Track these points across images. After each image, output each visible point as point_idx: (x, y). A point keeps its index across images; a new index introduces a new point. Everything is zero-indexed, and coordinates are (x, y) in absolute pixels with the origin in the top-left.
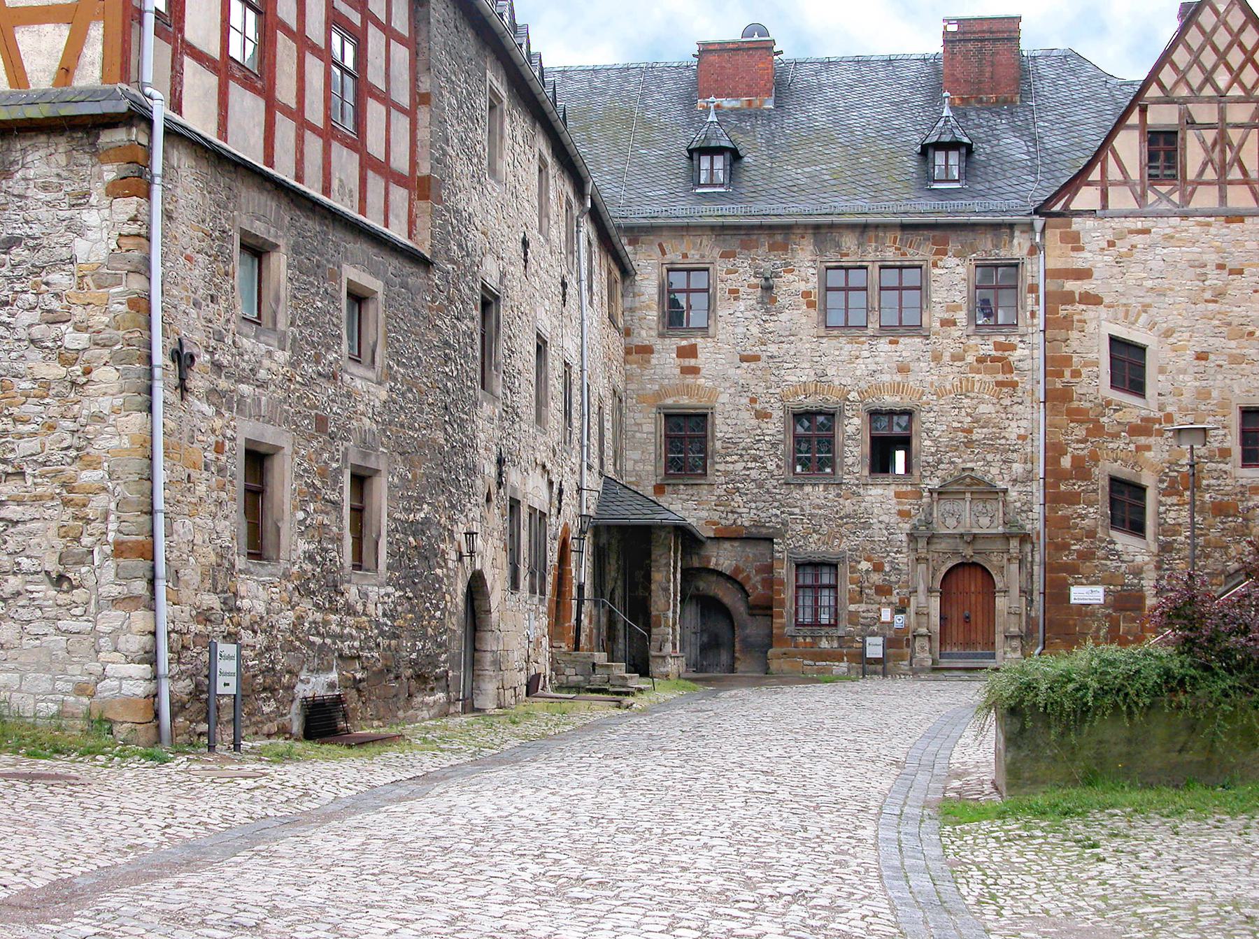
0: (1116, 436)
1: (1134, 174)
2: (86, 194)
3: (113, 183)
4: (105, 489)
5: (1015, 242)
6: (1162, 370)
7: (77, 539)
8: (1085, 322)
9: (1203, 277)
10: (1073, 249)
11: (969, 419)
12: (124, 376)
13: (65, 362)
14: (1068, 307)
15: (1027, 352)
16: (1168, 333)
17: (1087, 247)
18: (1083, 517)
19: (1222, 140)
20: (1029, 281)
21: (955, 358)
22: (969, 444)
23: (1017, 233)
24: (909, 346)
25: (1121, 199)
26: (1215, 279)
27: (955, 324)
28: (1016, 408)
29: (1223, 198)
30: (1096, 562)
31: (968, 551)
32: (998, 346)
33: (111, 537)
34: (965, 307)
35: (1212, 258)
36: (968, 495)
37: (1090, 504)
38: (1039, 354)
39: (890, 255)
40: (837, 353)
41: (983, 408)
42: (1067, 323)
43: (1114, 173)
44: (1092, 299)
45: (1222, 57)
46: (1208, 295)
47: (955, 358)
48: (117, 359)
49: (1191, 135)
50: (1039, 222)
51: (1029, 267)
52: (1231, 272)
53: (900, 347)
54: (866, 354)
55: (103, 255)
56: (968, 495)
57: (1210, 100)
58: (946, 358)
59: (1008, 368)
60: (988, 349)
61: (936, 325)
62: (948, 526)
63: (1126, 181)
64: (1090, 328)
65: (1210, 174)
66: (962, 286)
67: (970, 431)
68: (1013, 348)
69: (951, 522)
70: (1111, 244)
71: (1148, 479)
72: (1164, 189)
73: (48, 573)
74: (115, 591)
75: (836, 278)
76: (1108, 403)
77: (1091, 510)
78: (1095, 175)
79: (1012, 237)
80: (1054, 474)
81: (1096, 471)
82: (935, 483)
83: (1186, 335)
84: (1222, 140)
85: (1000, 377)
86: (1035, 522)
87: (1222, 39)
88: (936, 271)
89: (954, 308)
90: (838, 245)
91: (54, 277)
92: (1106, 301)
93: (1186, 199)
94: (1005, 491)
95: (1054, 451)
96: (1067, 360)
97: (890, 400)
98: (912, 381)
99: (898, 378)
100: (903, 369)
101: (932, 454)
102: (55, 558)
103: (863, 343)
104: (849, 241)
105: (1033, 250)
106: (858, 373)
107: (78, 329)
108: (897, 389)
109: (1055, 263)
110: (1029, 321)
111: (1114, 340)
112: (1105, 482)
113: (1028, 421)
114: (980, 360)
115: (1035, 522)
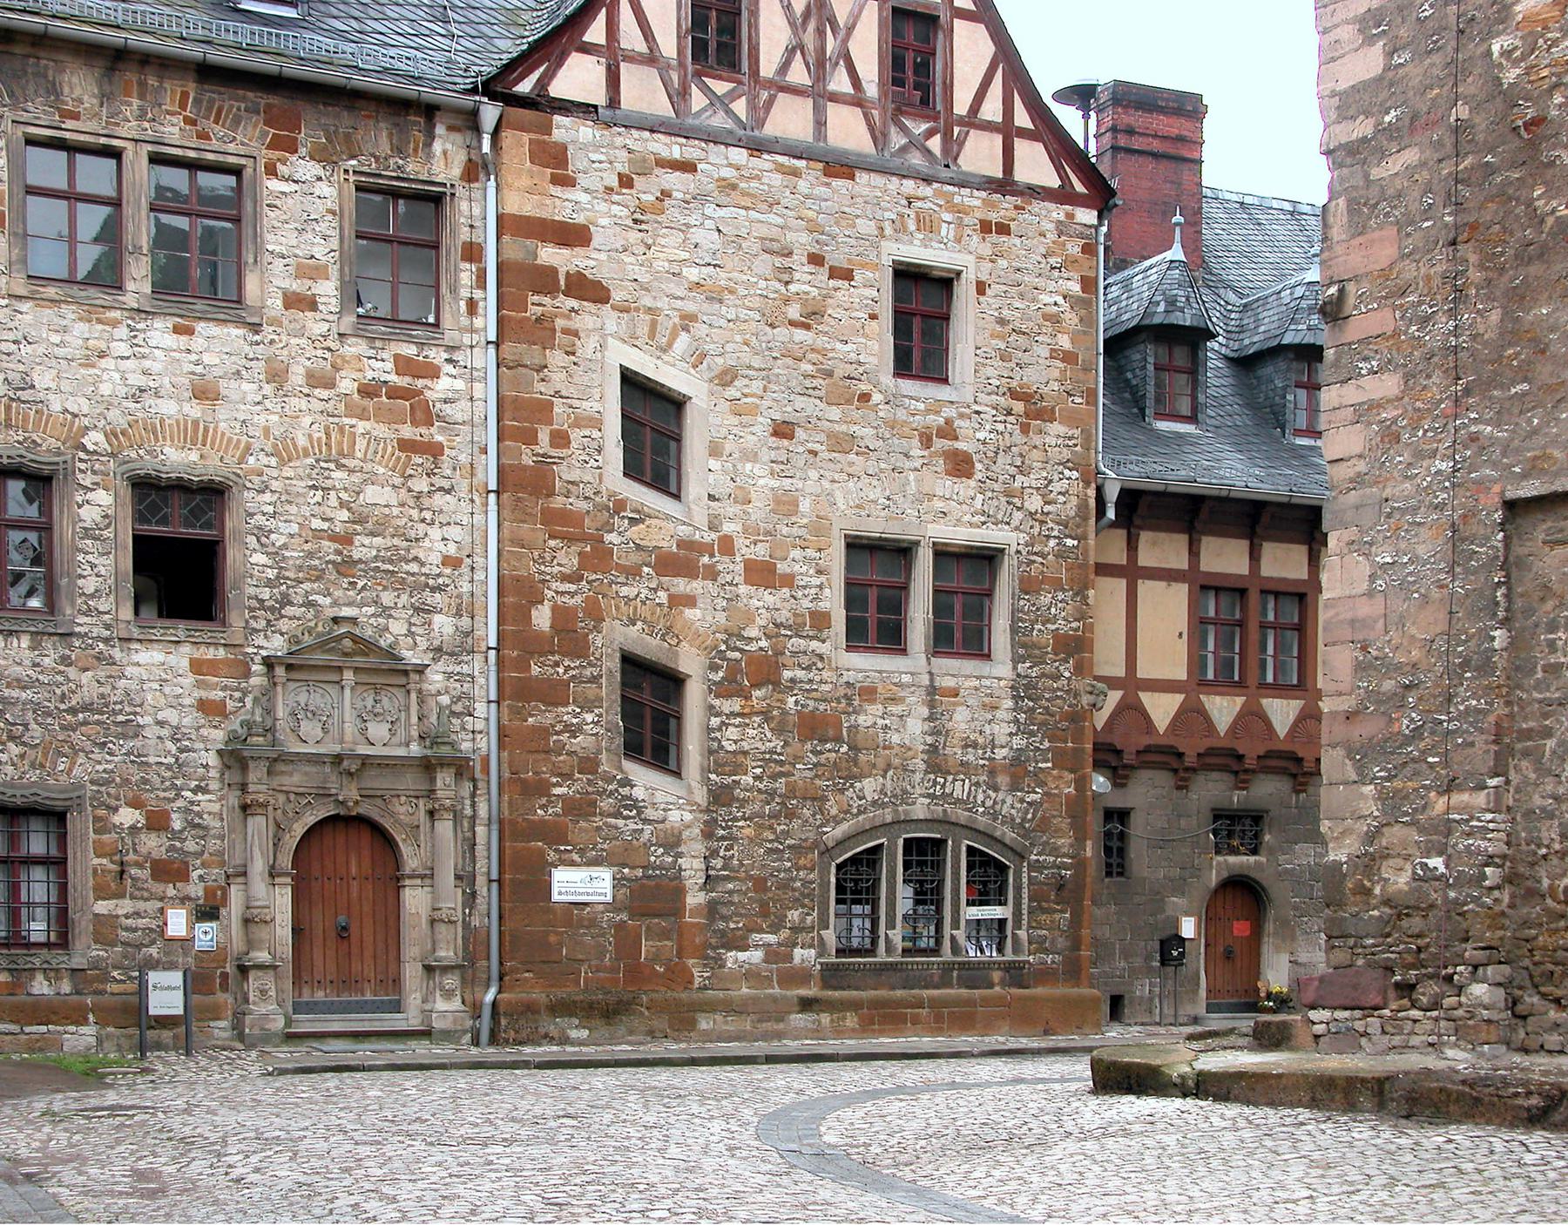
0: (633, 572)
1: (668, 46)
5: (437, 147)
6: (715, 451)
8: (576, 334)
9: (785, 275)
10: (558, 180)
11: (344, 515)
14: (546, 300)
15: (460, 384)
16: (726, 378)
17: (583, 180)
18: (574, 731)
20: (464, 235)
21: (319, 380)
22: (346, 566)
23: (440, 130)
24: (217, 343)
25: (643, 92)
26: (807, 281)
27: (312, 304)
28: (439, 500)
30: (598, 821)
31: (350, 792)
32: (404, 365)
34: (334, 271)
35: (801, 241)
36: (348, 675)
37: (587, 706)
38: (487, 392)
39: (174, 132)
40: (56, 338)
41: (372, 494)
42: (543, 332)
43: (631, 37)
44: (589, 290)
46: (794, 312)
47: (319, 380)
50: (490, 113)
51: (464, 206)
52: (834, 273)
53: (198, 343)
54: (122, 349)
56: (348, 675)
58: (297, 377)
59: (425, 414)
60: (382, 369)
61: (276, 303)
62: (311, 739)
63: (651, 58)
64: (587, 347)
66: (328, 226)
67: (346, 540)
68: (433, 372)
69: (310, 729)
70: (626, 182)
71: (690, 662)
72: (721, 87)
75: (48, 168)
76: (620, 506)
77: (589, 717)
78: (596, 33)
79: (431, 137)
80: (517, 642)
81: (598, 640)
82: (276, 645)
83: (756, 386)
85: (407, 432)
86: (478, 736)
88: (274, 185)
89: (312, 271)
90: (54, 91)
92: (617, 296)
94: (421, 670)
95: (517, 594)
96: (543, 410)
97: (177, 459)
98: (224, 419)
99: (194, 410)
100: (204, 392)
101: (270, 584)
103: (115, 323)
104: (80, 85)
105: (474, 171)
106: (105, 389)
108: (193, 434)
109: (518, 204)
110: (465, 321)
111: (631, 382)
112: (615, 664)
113: (462, 529)
114: (368, 391)
115: (478, 736)
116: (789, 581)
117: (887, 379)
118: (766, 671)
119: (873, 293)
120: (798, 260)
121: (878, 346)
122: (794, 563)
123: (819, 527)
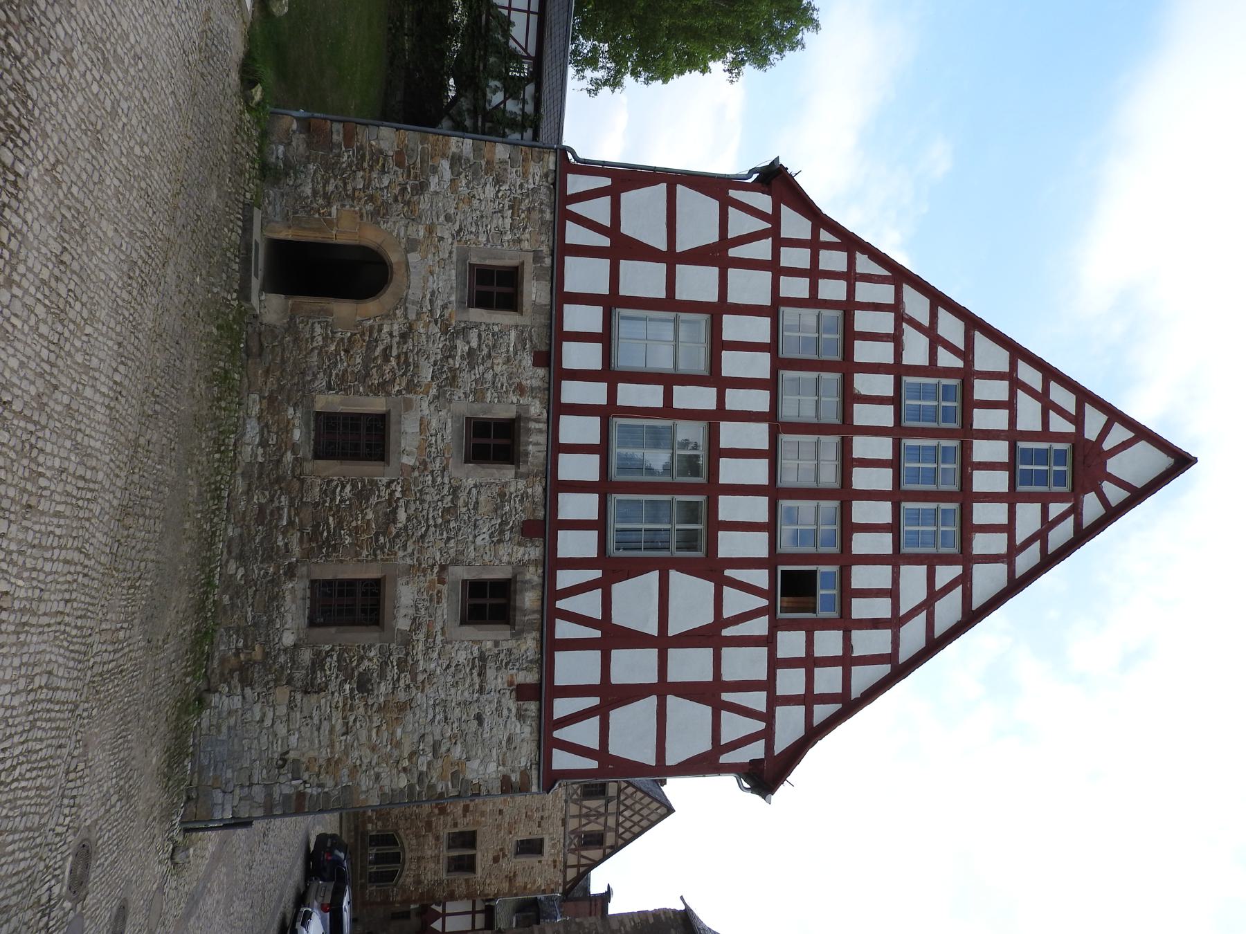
2: (504, 765)
3: (509, 778)
4: (336, 785)
7: (307, 769)
12: (402, 790)
13: (413, 754)
19: (599, 815)
26: (536, 816)
29: (574, 817)
33: (309, 791)
35: (546, 814)
45: (638, 812)
48: (411, 787)
49: (603, 802)
55: (469, 776)
57: (618, 808)
65: (585, 811)
73: (287, 752)
74: (276, 796)
84: (599, 815)
87: (645, 812)
91: (459, 747)
93: (575, 802)
102: (297, 757)
107: (429, 763)
116: (465, 816)
117: (516, 838)
118: (443, 811)
119: (536, 833)
120: (539, 815)
121: (523, 835)
122: (469, 818)
123: (478, 823)
